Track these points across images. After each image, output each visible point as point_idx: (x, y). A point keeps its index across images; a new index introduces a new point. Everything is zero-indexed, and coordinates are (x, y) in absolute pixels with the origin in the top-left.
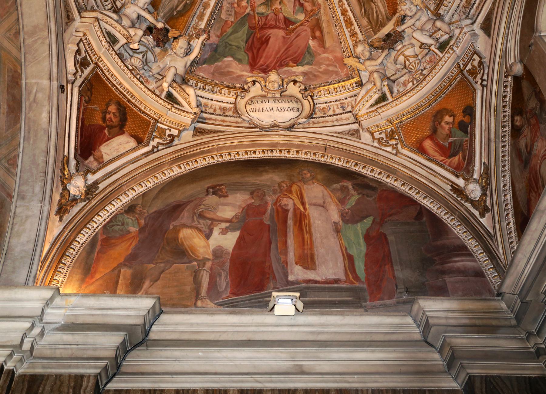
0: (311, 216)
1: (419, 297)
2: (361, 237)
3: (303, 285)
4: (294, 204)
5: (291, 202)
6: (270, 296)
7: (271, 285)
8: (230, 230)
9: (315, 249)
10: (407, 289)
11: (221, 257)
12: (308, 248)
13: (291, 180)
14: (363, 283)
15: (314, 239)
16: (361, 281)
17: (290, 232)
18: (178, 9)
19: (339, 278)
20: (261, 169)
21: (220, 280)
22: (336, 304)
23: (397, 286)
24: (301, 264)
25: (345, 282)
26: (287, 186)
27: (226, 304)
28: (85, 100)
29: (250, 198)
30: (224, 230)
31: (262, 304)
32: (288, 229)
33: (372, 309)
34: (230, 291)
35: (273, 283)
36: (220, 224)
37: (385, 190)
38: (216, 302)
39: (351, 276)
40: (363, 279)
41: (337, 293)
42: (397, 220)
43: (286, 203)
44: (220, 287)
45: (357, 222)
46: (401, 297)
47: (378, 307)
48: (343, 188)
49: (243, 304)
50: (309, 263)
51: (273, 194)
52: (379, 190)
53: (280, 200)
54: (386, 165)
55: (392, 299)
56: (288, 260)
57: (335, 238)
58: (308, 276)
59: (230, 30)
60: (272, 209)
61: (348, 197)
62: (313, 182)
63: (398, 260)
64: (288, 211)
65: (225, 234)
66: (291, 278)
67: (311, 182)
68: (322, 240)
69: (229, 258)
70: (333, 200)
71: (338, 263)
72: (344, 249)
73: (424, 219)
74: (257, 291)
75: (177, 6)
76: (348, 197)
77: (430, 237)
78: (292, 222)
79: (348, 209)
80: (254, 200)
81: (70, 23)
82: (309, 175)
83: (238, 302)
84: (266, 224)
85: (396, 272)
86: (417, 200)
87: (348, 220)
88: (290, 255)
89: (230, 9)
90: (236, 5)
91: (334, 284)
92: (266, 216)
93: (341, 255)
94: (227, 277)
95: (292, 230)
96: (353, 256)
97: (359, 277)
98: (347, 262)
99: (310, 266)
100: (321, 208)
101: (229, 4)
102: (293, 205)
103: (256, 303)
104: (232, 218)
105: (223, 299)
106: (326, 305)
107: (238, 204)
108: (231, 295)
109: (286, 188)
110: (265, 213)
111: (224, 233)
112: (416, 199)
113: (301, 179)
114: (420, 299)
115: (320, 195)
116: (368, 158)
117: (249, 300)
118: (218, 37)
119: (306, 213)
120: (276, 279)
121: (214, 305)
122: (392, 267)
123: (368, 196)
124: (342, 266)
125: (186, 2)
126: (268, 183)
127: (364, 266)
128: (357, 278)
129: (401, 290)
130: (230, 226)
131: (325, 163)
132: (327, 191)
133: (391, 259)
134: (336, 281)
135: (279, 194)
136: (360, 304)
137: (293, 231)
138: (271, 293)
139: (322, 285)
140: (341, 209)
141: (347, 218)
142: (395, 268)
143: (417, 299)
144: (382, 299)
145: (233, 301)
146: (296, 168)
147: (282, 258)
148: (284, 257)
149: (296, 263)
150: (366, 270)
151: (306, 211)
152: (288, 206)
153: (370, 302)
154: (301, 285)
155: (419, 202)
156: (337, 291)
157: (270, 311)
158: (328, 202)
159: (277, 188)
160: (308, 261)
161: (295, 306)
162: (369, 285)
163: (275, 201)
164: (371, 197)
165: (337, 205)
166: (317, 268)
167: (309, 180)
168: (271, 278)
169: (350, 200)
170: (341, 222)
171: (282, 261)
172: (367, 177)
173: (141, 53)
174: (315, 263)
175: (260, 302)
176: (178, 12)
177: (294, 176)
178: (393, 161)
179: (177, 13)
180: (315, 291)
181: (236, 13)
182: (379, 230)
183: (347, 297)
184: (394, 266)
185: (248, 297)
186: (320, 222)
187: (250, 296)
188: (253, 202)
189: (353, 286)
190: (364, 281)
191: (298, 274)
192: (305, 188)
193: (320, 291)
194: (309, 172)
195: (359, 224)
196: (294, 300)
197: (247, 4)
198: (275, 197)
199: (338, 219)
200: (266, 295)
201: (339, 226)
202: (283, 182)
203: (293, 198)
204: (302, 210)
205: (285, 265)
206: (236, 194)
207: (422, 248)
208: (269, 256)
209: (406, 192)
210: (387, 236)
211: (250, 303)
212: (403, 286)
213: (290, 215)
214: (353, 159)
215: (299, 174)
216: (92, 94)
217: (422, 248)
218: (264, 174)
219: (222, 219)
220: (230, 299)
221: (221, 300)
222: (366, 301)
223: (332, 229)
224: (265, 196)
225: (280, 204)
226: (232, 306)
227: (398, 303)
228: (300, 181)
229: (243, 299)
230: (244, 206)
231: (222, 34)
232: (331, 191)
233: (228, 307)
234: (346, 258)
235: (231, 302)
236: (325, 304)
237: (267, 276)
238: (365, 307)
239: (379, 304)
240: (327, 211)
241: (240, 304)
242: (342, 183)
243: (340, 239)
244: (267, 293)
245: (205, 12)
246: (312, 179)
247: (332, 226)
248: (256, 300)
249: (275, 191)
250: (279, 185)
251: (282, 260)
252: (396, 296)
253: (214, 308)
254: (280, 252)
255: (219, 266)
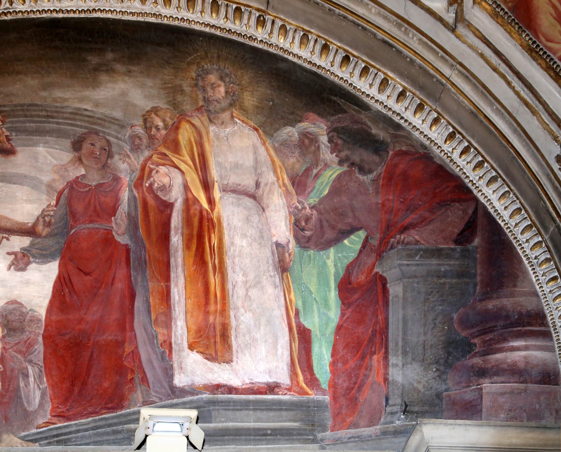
0: (225, 224)
1: (426, 421)
2: (333, 284)
3: (204, 396)
4: (186, 187)
5: (178, 180)
6: (137, 420)
7: (138, 395)
8: (34, 257)
9: (232, 314)
10: (406, 406)
11: (23, 330)
12: (216, 311)
13: (175, 105)
14: (324, 392)
15: (230, 286)
16: (321, 389)
17: (177, 266)
19: (279, 381)
20: (94, 60)
21: (27, 385)
22: (266, 435)
23: (387, 400)
24: (201, 350)
25: (289, 390)
26: (166, 127)
27: (46, 438)
29: (72, 162)
30: (20, 255)
31: (119, 436)
32: (172, 260)
33: (334, 444)
34: (53, 410)
35: (142, 393)
36: (8, 239)
37: (405, 153)
38: (23, 434)
39: (301, 378)
40: (325, 386)
41: (272, 414)
42: (417, 242)
43: (166, 180)
44: (28, 402)
45: (326, 245)
46: (392, 422)
47: (345, 440)
48: (307, 141)
49: (82, 437)
50: (219, 346)
51: (132, 150)
52: (391, 153)
53: (151, 170)
54: (421, 67)
55: (374, 425)
56: (173, 341)
57: (276, 287)
58: (216, 375)
60: (132, 199)
61: (315, 171)
62: (232, 117)
63: (400, 344)
64: (169, 206)
65: (23, 269)
66: (180, 380)
67: (226, 115)
68: (247, 290)
69: (42, 332)
70: (278, 179)
71: (279, 347)
72: (292, 315)
73: (477, 241)
74: (108, 409)
76: (315, 171)
77: (478, 288)
78: (180, 242)
79: (312, 208)
80: (85, 167)
82: (222, 90)
83: (70, 433)
84: (119, 243)
85: (391, 370)
86: (473, 188)
87: (309, 239)
88: (176, 326)
91: (266, 393)
92: (119, 221)
93: (287, 329)
94: (40, 377)
95: (180, 260)
96: (309, 331)
97: (317, 380)
98: (296, 345)
99: (219, 354)
100: (248, 202)
102: (182, 188)
103: (107, 434)
104: (35, 224)
105: (37, 428)
106: (248, 437)
107: (46, 178)
108: (55, 420)
109: (164, 132)
110: (113, 211)
111: (21, 266)
112: (470, 185)
113: (201, 103)
114: (425, 424)
115: (249, 161)
116: (380, 35)
117: (93, 429)
119: (215, 216)
120: (148, 383)
121: (20, 441)
122: (386, 358)
123: (362, 170)
124: (287, 354)
126: (118, 114)
127: (330, 355)
128: (313, 381)
129: (395, 409)
130: (32, 245)
131: (266, 48)
132: (267, 150)
133: (387, 340)
134: (272, 388)
135: (147, 153)
136: (313, 435)
137: (184, 265)
138: (139, 412)
139: (243, 397)
140: (296, 208)
141: (308, 233)
142: (392, 360)
143: (420, 425)
144: (356, 426)
145: (60, 432)
146: (189, 64)
147: (161, 332)
148: (165, 332)
149: (191, 347)
150: (333, 364)
151: (212, 210)
152: (170, 191)
153: (332, 431)
154: (199, 396)
155: (475, 192)
156: (271, 410)
157: (139, 448)
158: (266, 184)
159: (140, 130)
160: (215, 342)
161: (187, 437)
162: (335, 398)
163: (137, 174)
164: (370, 171)
165: (287, 193)
166: (235, 358)
167: (223, 110)
168: (137, 381)
169: (319, 181)
170: (292, 245)
171: (159, 342)
172: (365, 107)
174: (230, 347)
175: (115, 432)
177: (182, 92)
178: (441, 53)
180: (228, 410)
182: (373, 267)
183: (290, 421)
184: (390, 357)
185: (91, 422)
186: (244, 243)
187: (95, 421)
188: (83, 176)
189: (305, 398)
190: (327, 388)
191: (193, 373)
192: (212, 134)
193: (237, 410)
194: (221, 79)
195: (332, 251)
196: (187, 425)
198: (137, 161)
199: (288, 234)
200: (129, 418)
201: (287, 255)
202: (155, 110)
203: (183, 166)
204: (205, 205)
205: (167, 351)
206: (35, 144)
207: (455, 316)
208: (132, 329)
209: (452, 160)
210: (388, 285)
211: (95, 434)
212: (399, 401)
213: (176, 220)
214: (340, 41)
215: (196, 85)
217: (455, 316)
218: (104, 77)
219: (9, 225)
220: (52, 426)
221: (35, 431)
222: (324, 430)
223: (271, 261)
224: (110, 155)
225: (151, 185)
226: (59, 443)
227: (385, 433)
228: (199, 109)
229: (81, 428)
230: (60, 186)
232: (276, 150)
233: (49, 444)
234: (296, 335)
235: (55, 433)
236: (246, 435)
237: (129, 377)
238: (322, 440)
239: (349, 436)
240: (264, 210)
241: (76, 437)
242: (304, 125)
243: (286, 291)
244: (129, 414)
246: (231, 105)
247: (273, 254)
248: (109, 429)
249: (137, 141)
250: (145, 121)
251: (161, 338)
252: (382, 420)
253: (20, 447)
254: (156, 320)
255: (20, 352)
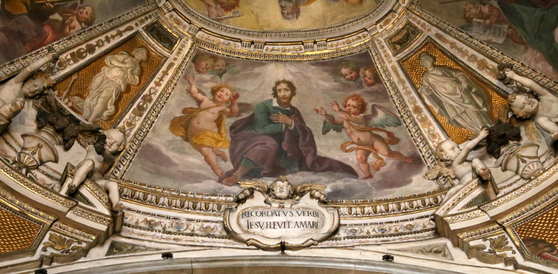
18: (481, 104)
28: (548, 252)
59: (520, 32)
75: (477, 106)
81: (447, 251)
89: (492, 29)
90: (488, 22)
101: (485, 31)
118: (526, 49)
125: (475, 93)
173: (518, 164)
176: (485, 105)
179: (486, 107)
181: (498, 22)
197: (487, 5)
216: (544, 241)
231: (523, 43)
245: (491, 67)
